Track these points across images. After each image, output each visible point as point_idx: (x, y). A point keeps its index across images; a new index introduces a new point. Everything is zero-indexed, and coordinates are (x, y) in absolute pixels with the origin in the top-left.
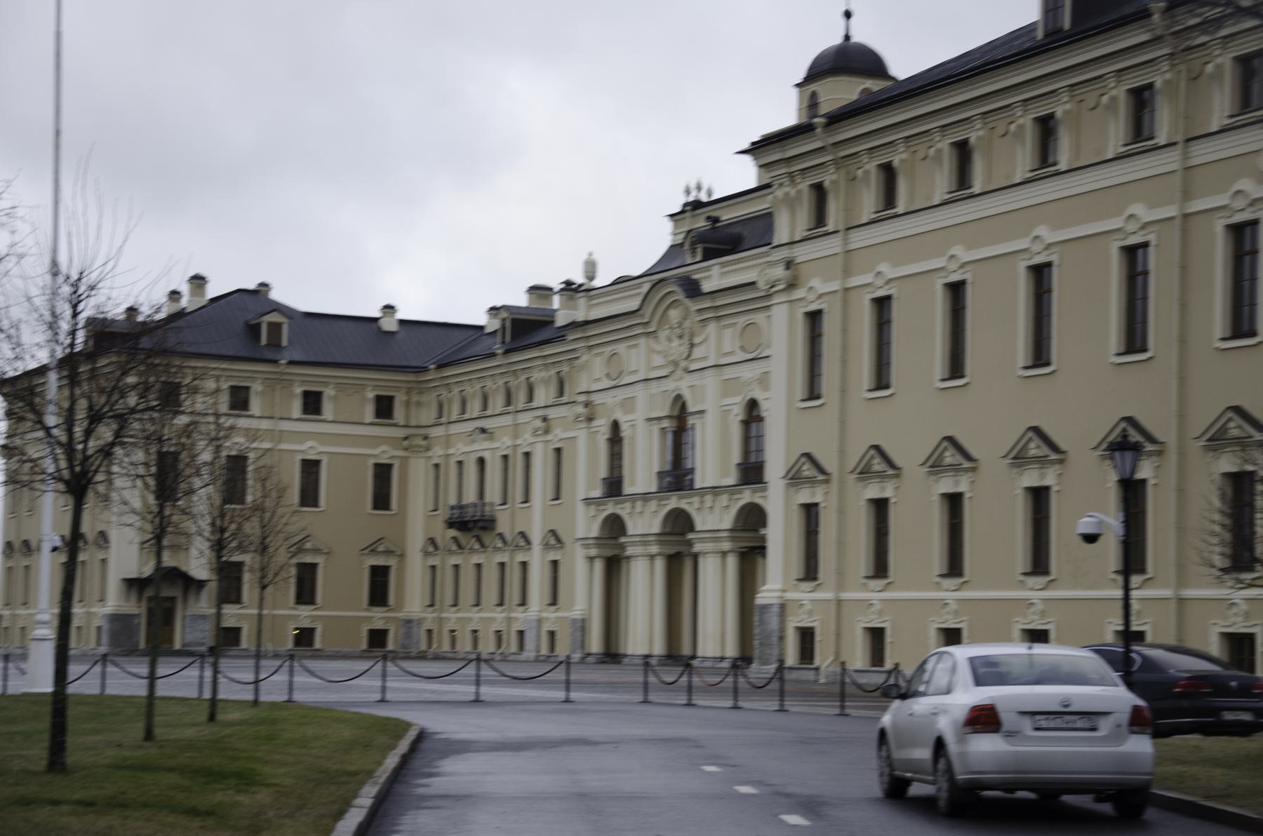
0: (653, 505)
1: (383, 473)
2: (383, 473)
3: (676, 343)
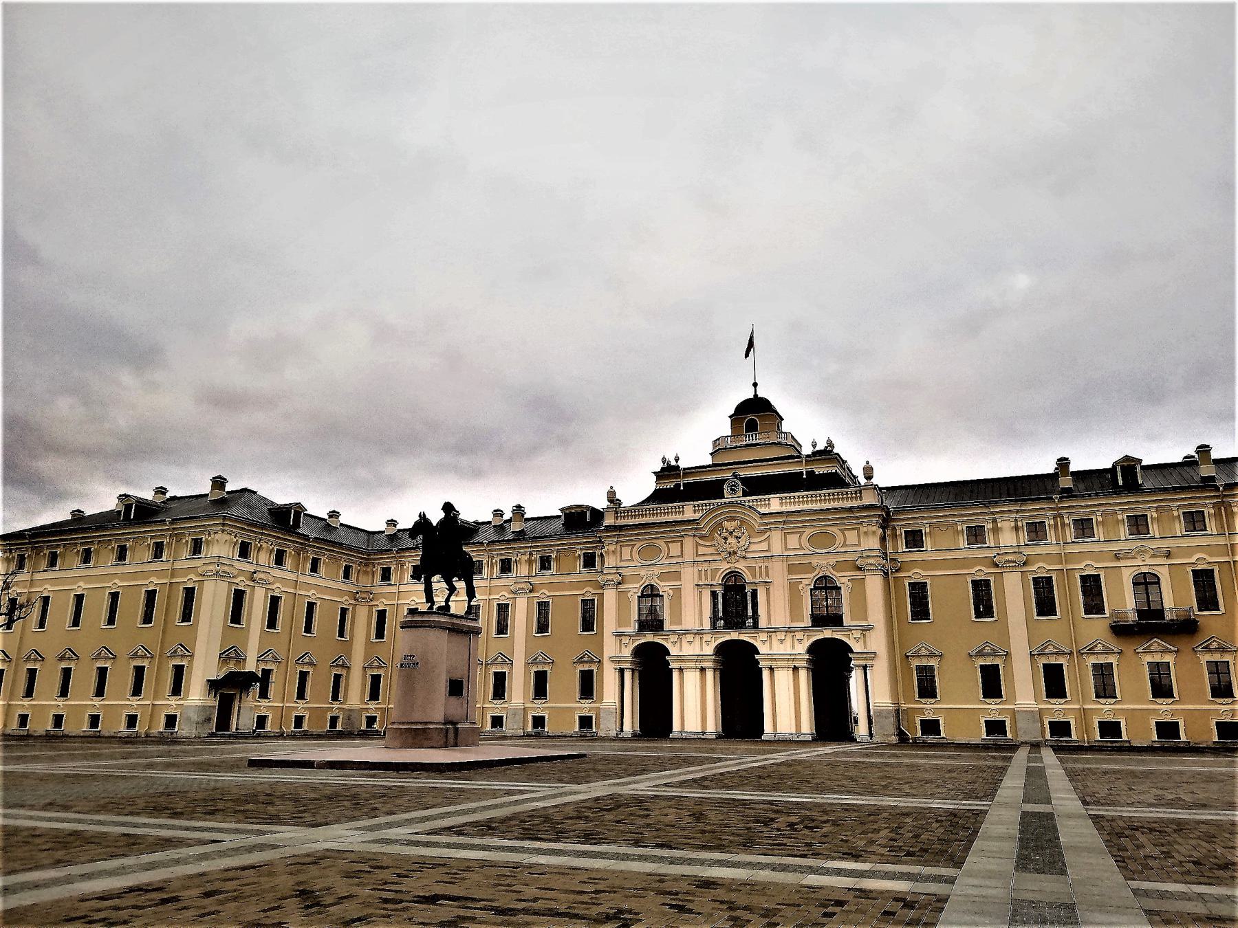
0: (707, 637)
1: (344, 611)
2: (344, 611)
3: (731, 540)
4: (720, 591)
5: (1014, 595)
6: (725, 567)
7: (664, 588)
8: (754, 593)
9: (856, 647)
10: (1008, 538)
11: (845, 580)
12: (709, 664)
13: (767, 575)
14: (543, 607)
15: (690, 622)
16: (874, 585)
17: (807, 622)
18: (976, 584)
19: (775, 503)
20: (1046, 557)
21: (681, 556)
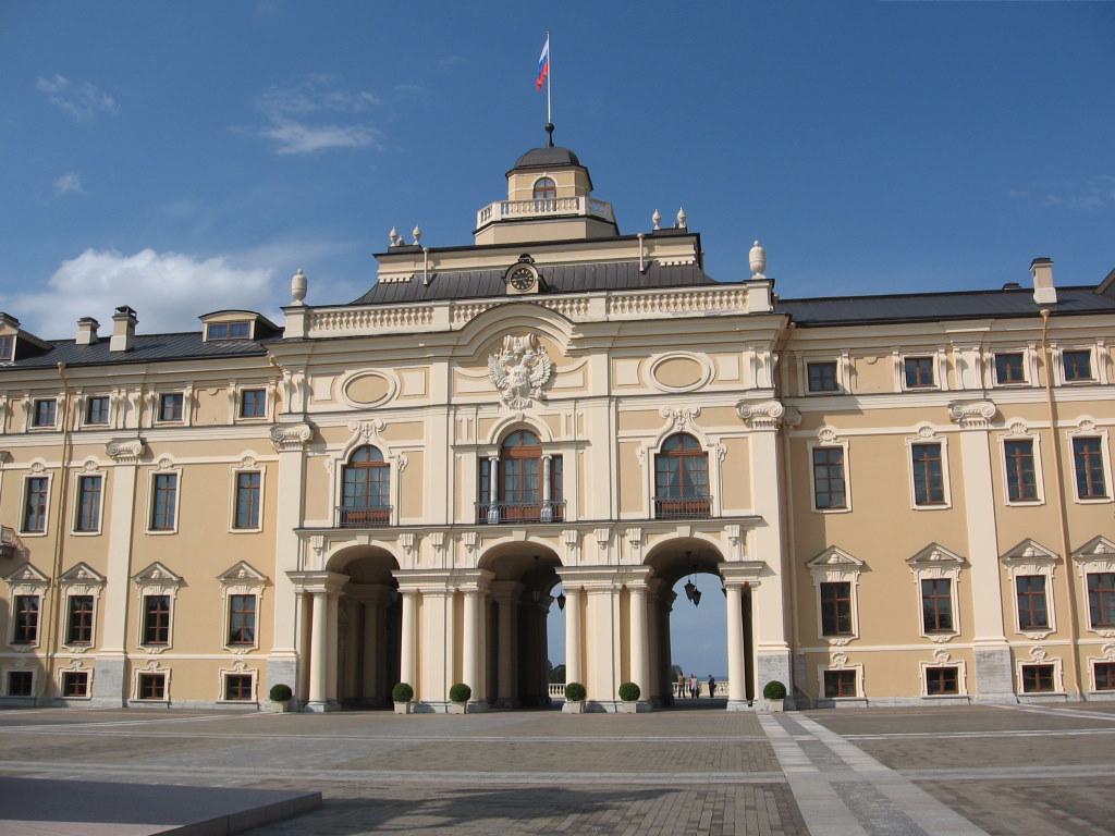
0: (469, 538)
4: (493, 454)
5: (974, 468)
6: (506, 415)
7: (389, 450)
8: (556, 461)
10: (971, 378)
11: (715, 439)
12: (473, 586)
13: (579, 429)
14: (163, 485)
15: (433, 513)
16: (762, 451)
17: (646, 510)
18: (918, 449)
19: (595, 308)
20: (1025, 414)
21: (425, 394)
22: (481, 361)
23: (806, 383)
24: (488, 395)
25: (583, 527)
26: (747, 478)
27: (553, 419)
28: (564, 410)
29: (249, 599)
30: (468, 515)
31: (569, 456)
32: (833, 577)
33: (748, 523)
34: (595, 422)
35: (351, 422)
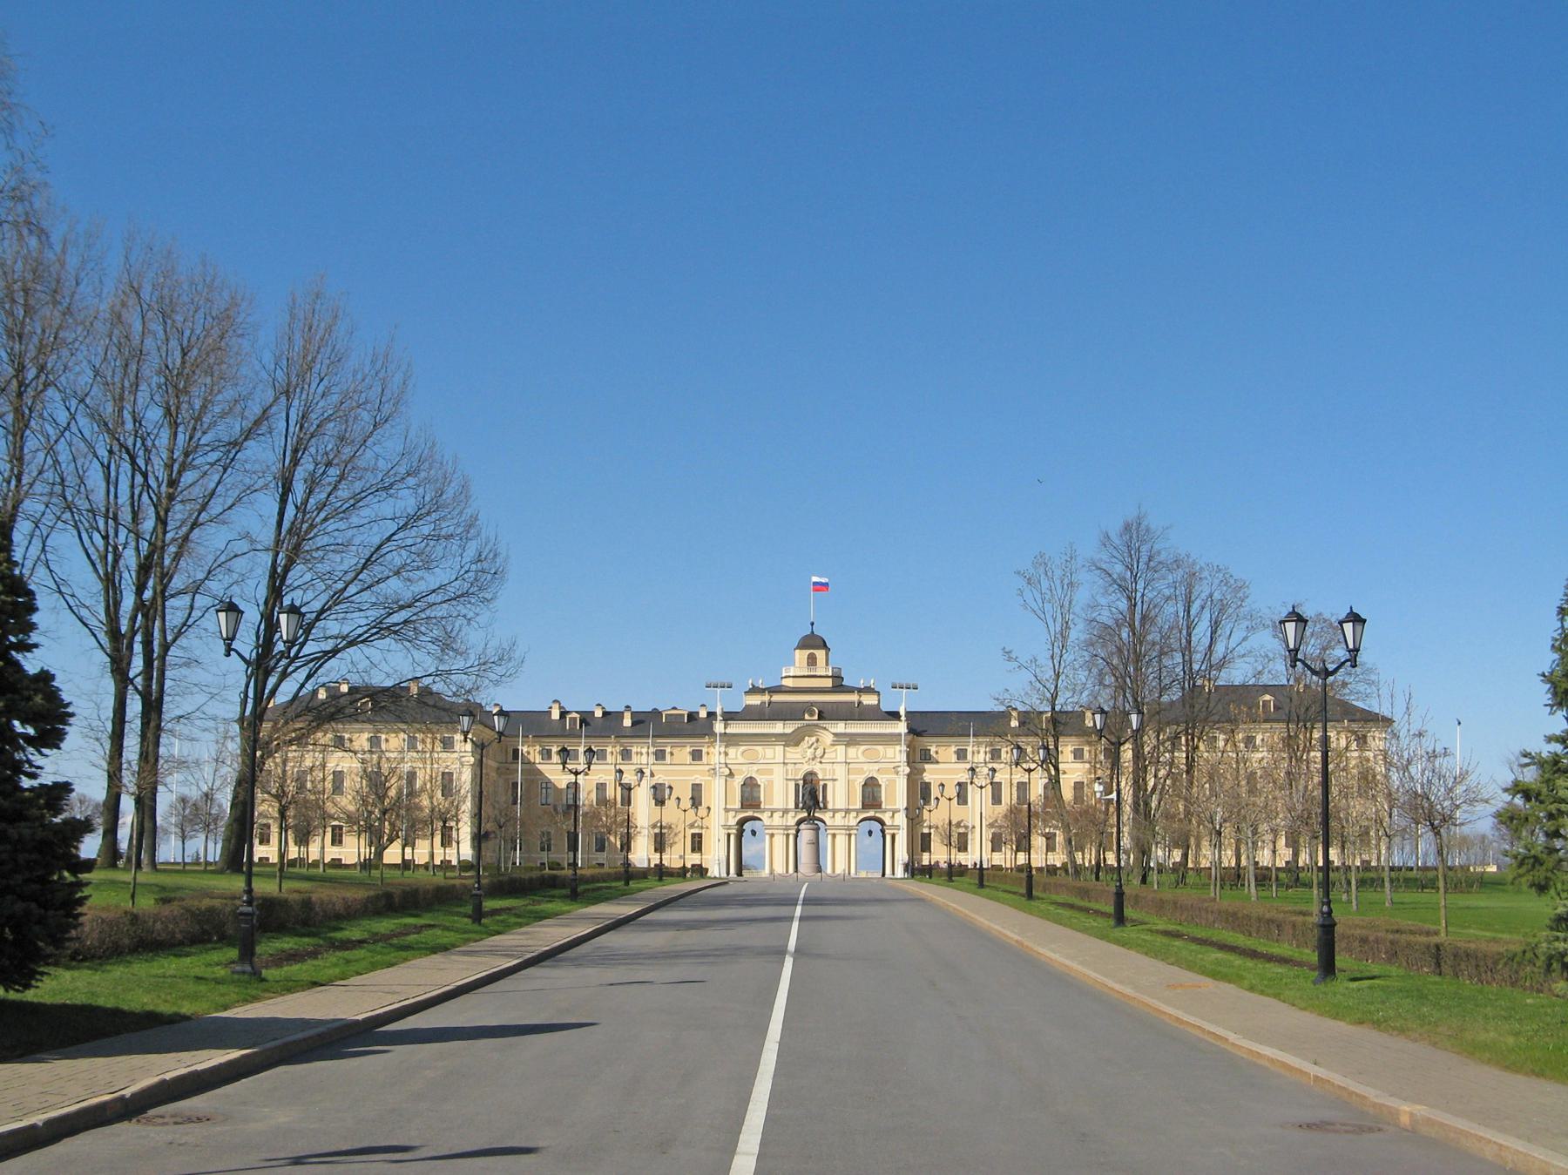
0: (792, 814)
6: (806, 768)
7: (761, 780)
8: (825, 787)
9: (888, 821)
16: (901, 785)
17: (859, 805)
19: (840, 727)
22: (797, 744)
23: (918, 758)
24: (801, 759)
25: (835, 811)
26: (896, 795)
27: (824, 770)
28: (828, 767)
29: (700, 835)
30: (792, 805)
31: (830, 785)
32: (926, 831)
33: (894, 812)
34: (840, 772)
35: (744, 768)
